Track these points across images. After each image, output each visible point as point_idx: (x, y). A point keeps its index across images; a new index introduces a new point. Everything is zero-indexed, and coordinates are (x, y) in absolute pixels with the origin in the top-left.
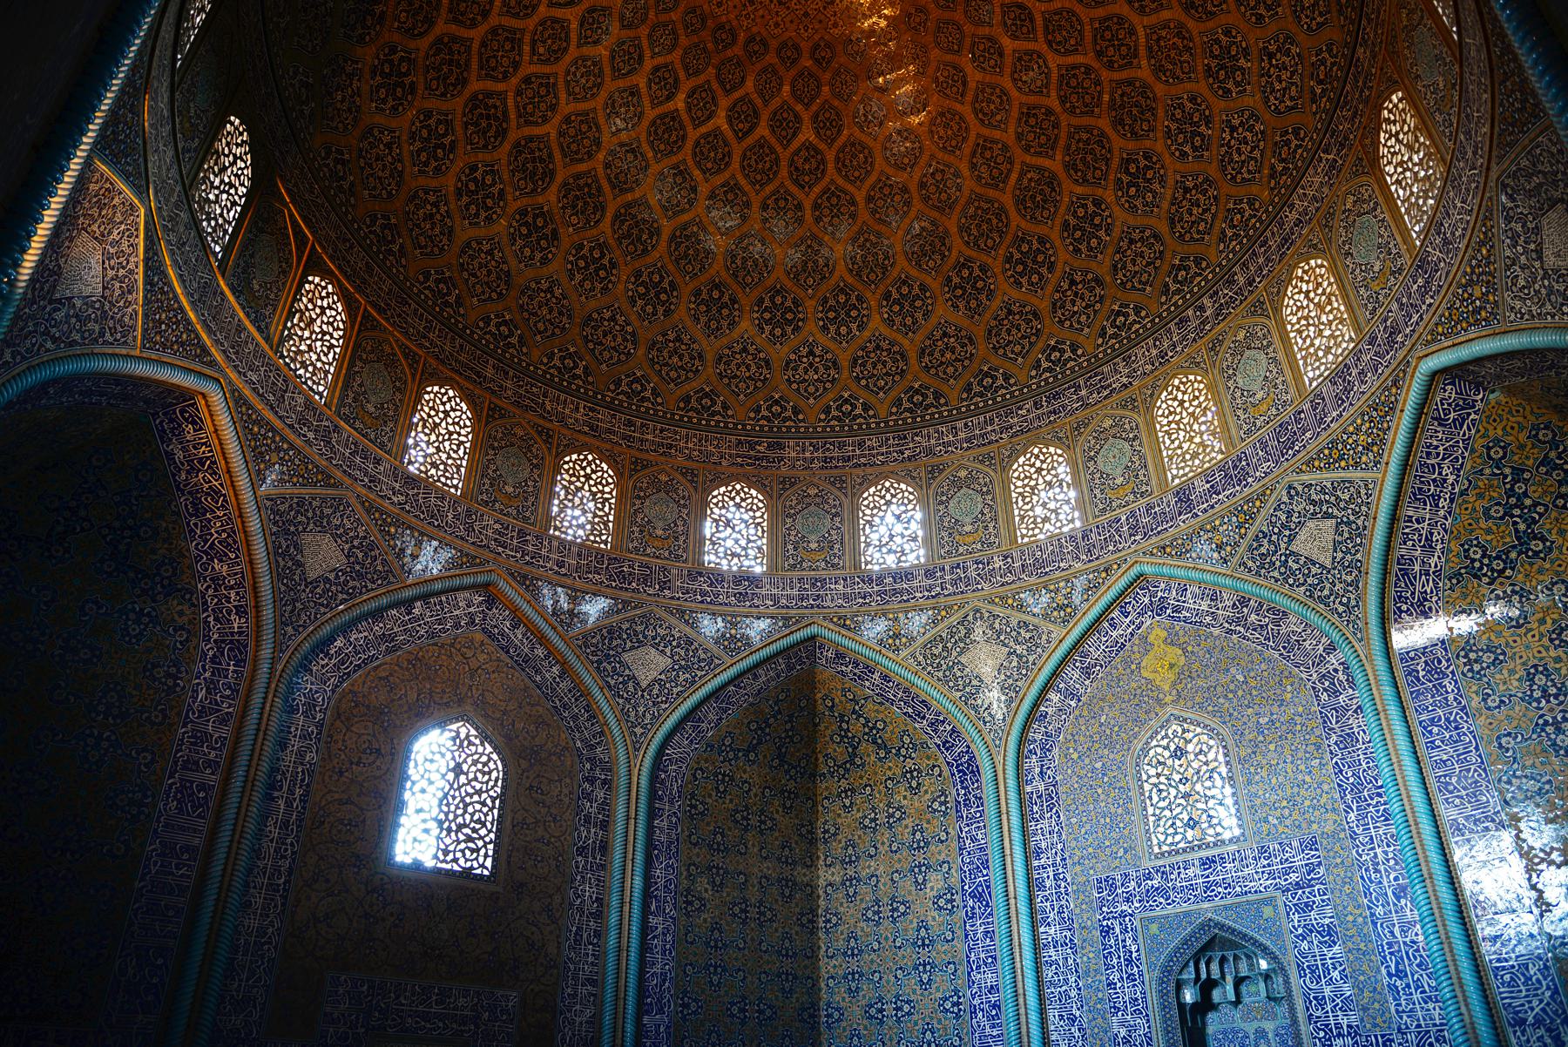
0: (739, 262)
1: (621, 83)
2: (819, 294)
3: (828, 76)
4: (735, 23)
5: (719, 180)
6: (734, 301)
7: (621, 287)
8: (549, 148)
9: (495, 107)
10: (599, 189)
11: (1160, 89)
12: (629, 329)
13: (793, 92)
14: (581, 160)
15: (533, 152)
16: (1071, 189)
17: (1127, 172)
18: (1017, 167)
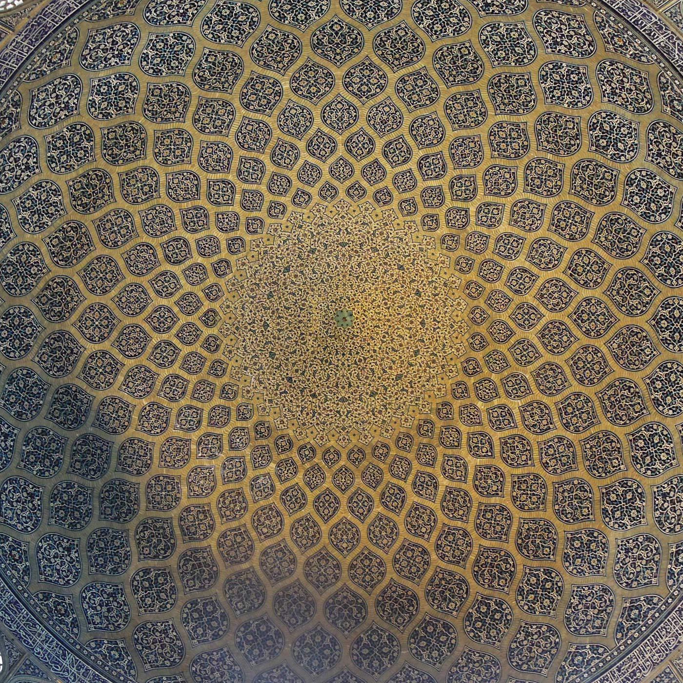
0: (569, 510)
1: (404, 512)
2: (629, 460)
3: (486, 370)
4: (423, 417)
5: (508, 487)
6: (591, 534)
7: (517, 611)
8: (399, 585)
9: (345, 597)
10: (451, 574)
11: (541, 108)
12: (544, 628)
13: (484, 400)
14: (425, 571)
15: (391, 597)
16: (617, 205)
17: (605, 148)
18: (595, 248)
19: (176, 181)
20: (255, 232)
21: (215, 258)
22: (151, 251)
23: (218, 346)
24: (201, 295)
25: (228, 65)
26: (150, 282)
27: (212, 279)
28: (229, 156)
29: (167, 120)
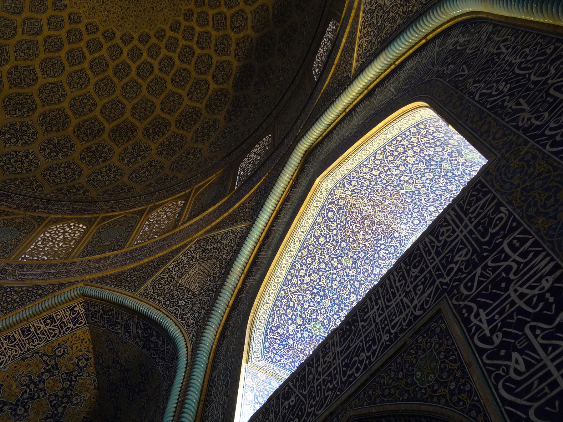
19: (103, 93)
20: (113, 33)
21: (140, 46)
22: (151, 84)
23: (188, 11)
24: (164, 41)
25: (12, 103)
26: (168, 75)
27: (153, 40)
28: (73, 74)
29: (67, 116)
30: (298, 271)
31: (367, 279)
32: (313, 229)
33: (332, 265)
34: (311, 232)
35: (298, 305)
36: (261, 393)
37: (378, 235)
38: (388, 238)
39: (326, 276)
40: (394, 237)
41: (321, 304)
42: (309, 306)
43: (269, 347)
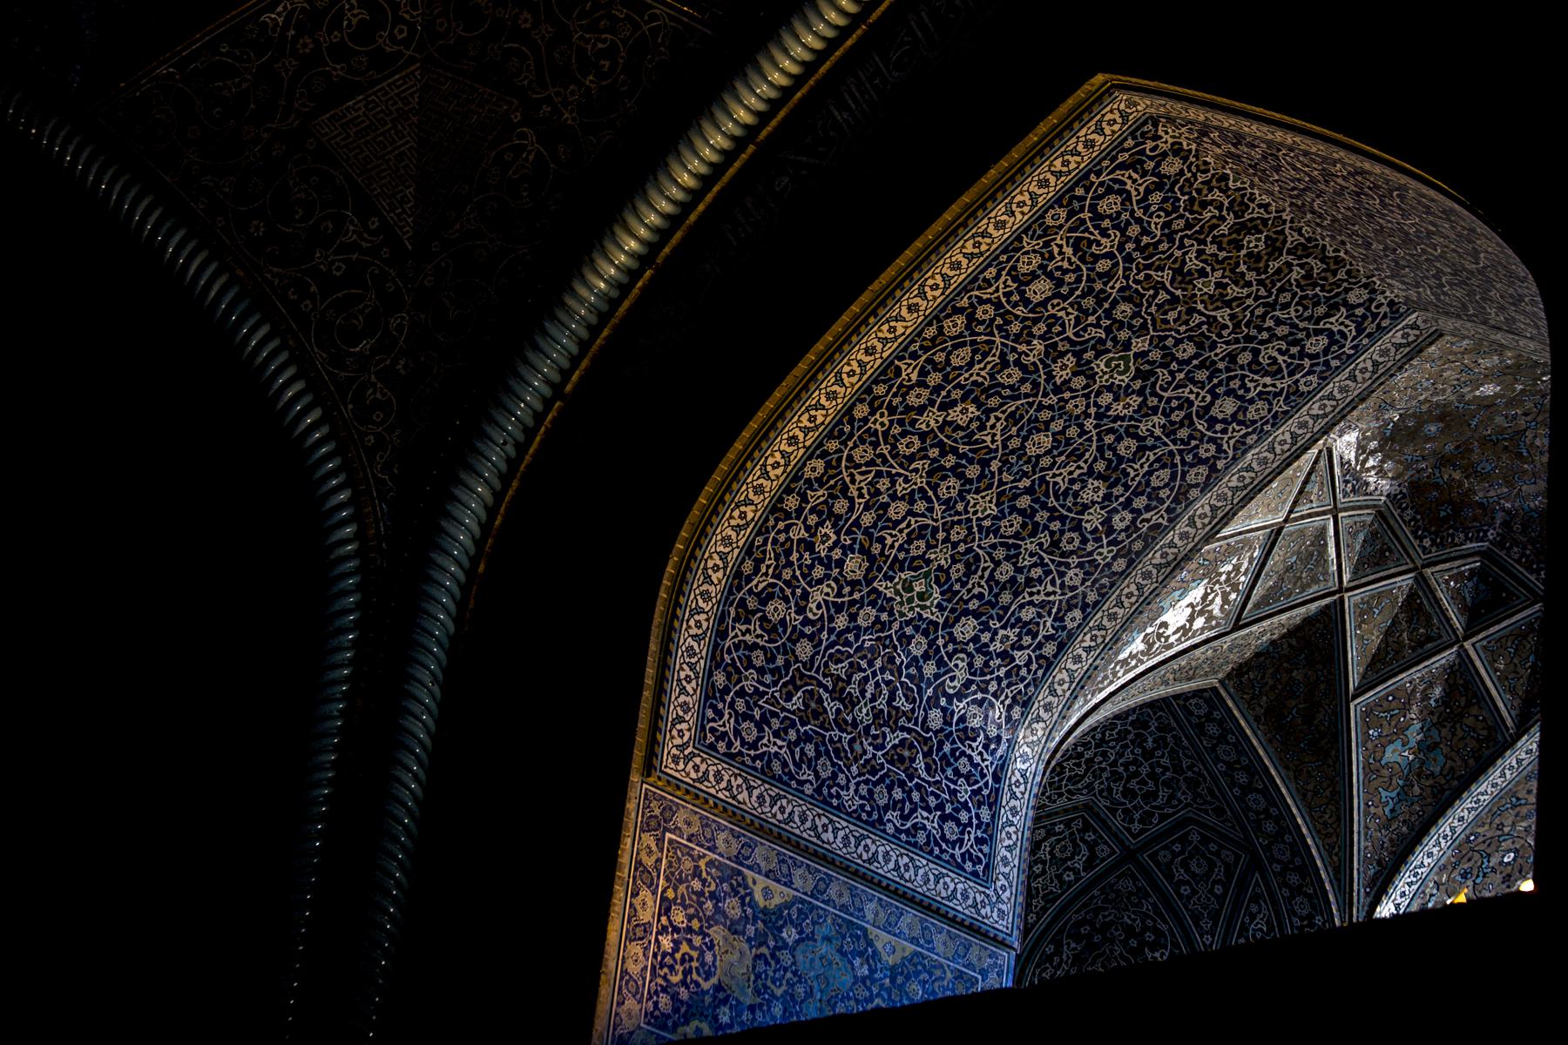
30: (905, 390)
31: (1174, 432)
32: (1017, 250)
33: (1050, 377)
34: (1004, 258)
35: (867, 508)
36: (682, 888)
37: (1282, 290)
38: (1317, 304)
39: (1012, 414)
40: (1345, 303)
41: (960, 507)
42: (910, 513)
43: (726, 690)
